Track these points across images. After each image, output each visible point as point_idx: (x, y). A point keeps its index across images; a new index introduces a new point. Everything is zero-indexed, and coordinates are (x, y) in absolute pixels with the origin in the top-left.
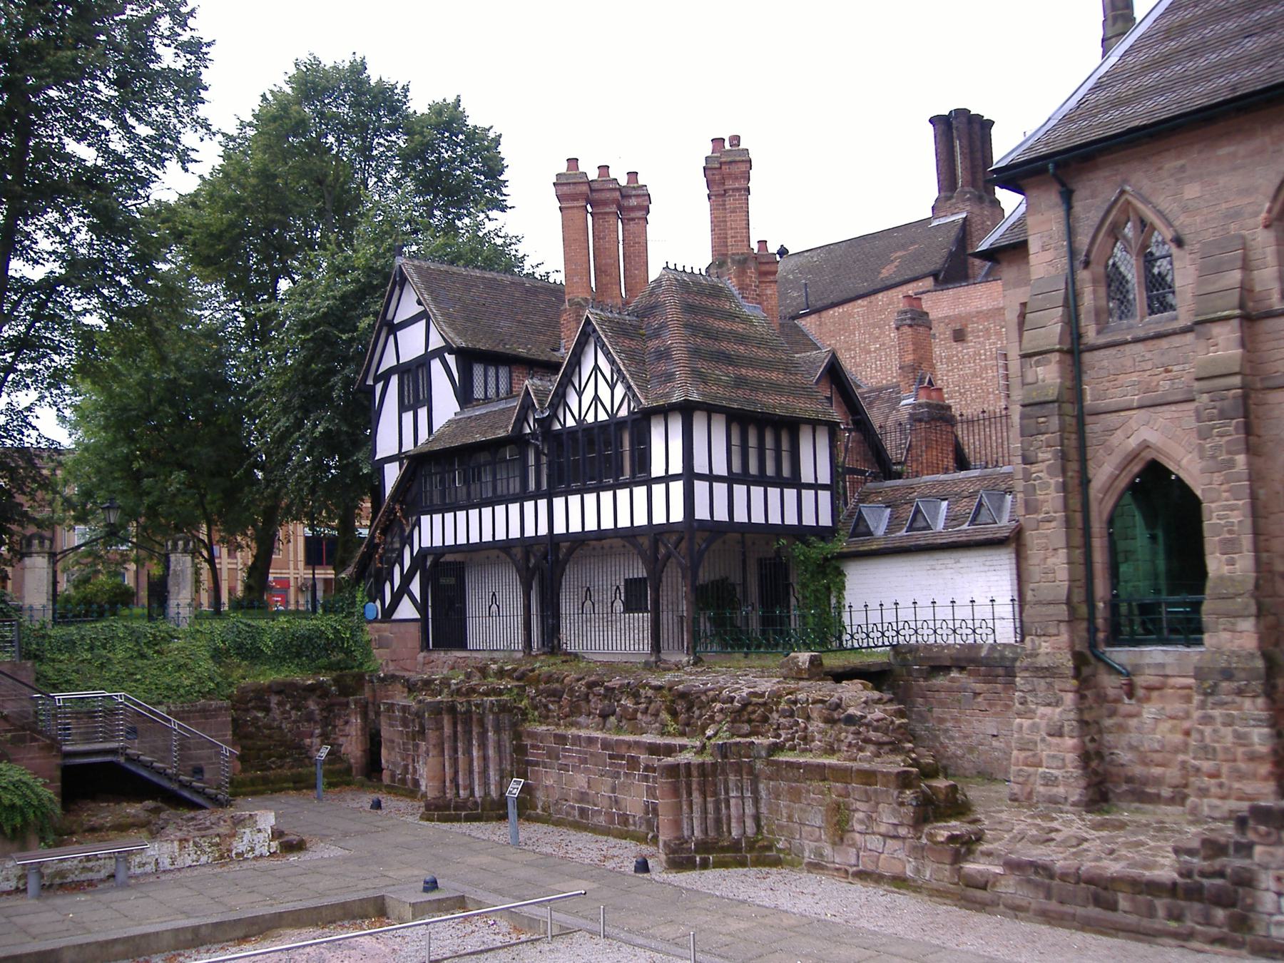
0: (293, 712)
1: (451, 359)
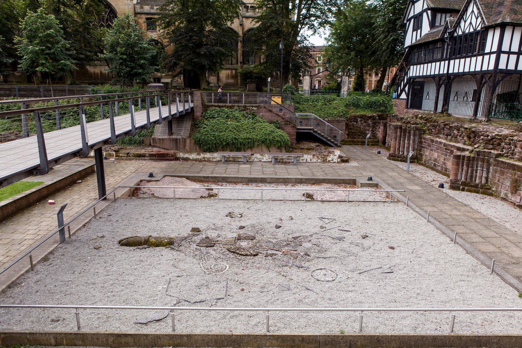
1: (429, 12)
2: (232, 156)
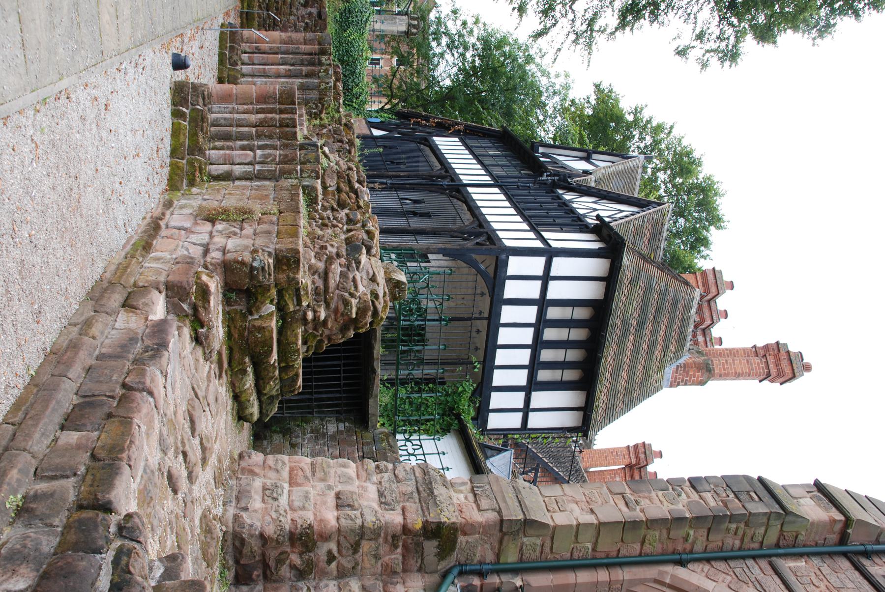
0: (303, 24)
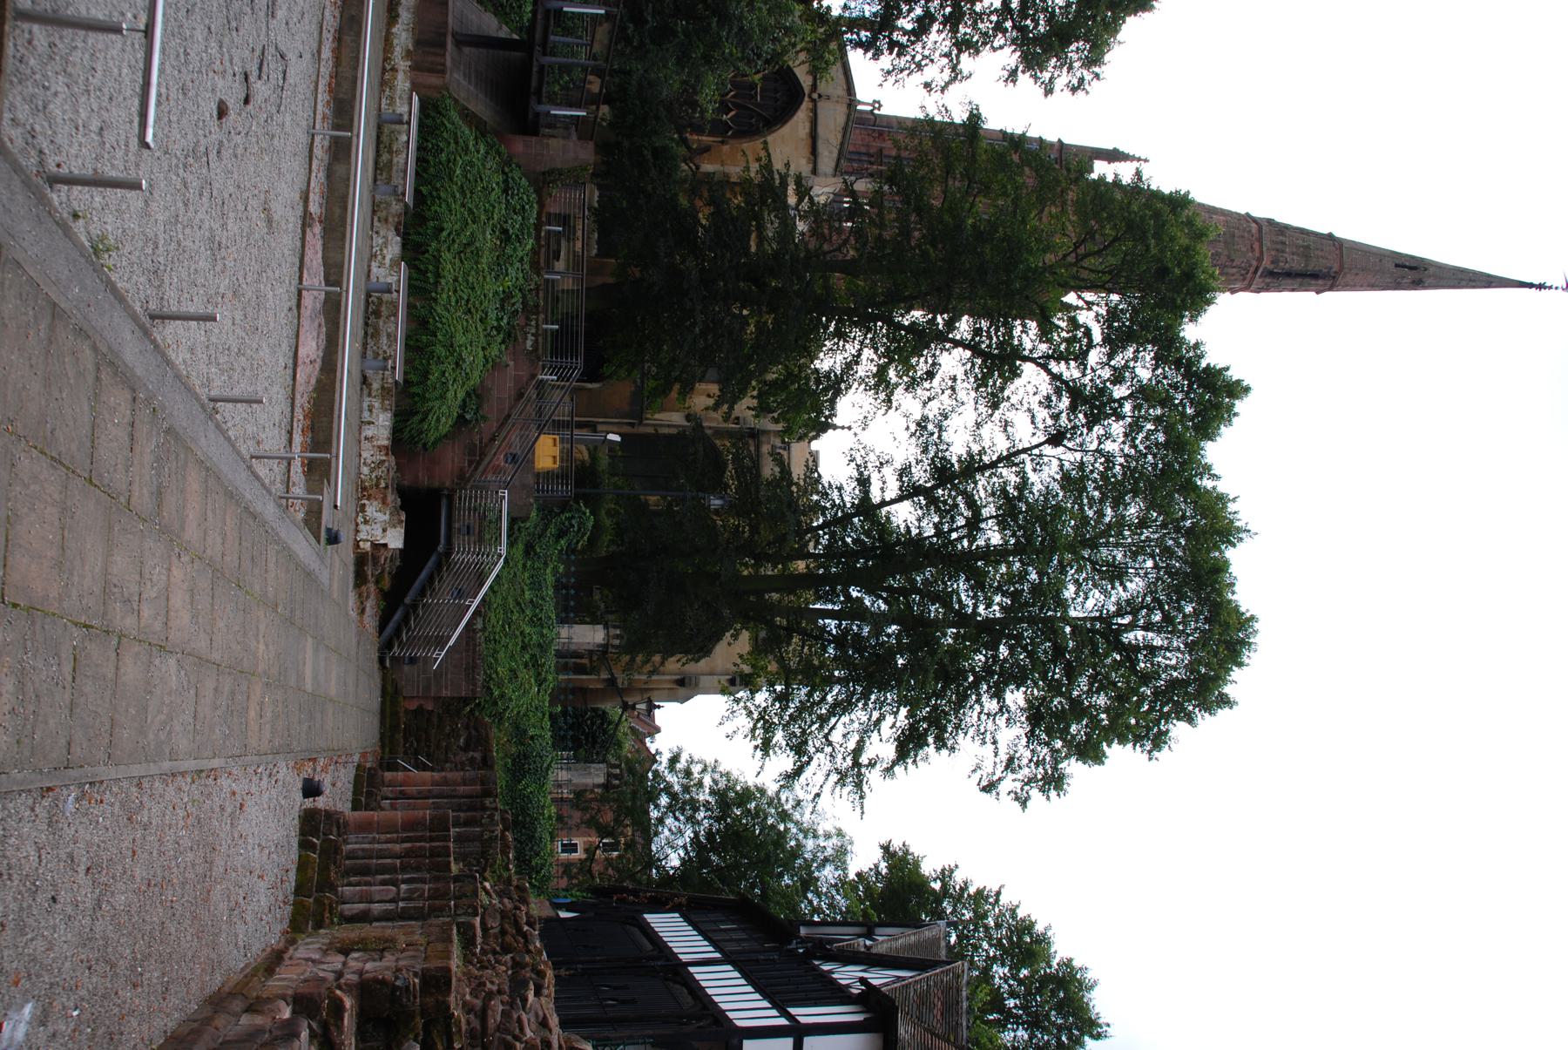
2: (395, 160)
